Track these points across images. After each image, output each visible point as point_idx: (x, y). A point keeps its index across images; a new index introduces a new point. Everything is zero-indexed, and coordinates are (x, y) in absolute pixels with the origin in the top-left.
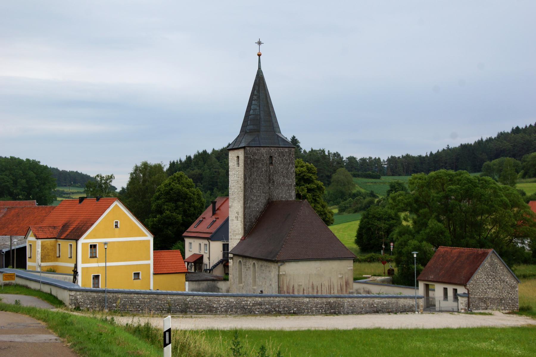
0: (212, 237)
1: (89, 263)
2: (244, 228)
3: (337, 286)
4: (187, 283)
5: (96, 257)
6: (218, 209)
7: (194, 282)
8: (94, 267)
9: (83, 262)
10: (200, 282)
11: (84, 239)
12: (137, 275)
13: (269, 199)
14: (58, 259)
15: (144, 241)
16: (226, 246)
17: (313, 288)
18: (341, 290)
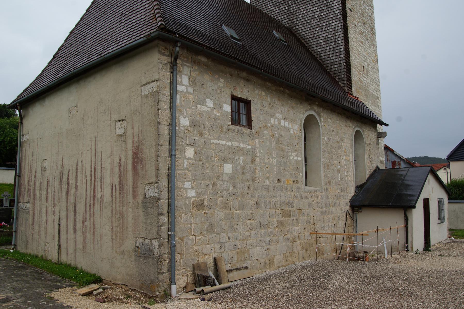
3: (112, 169)
17: (61, 181)
18: (121, 183)
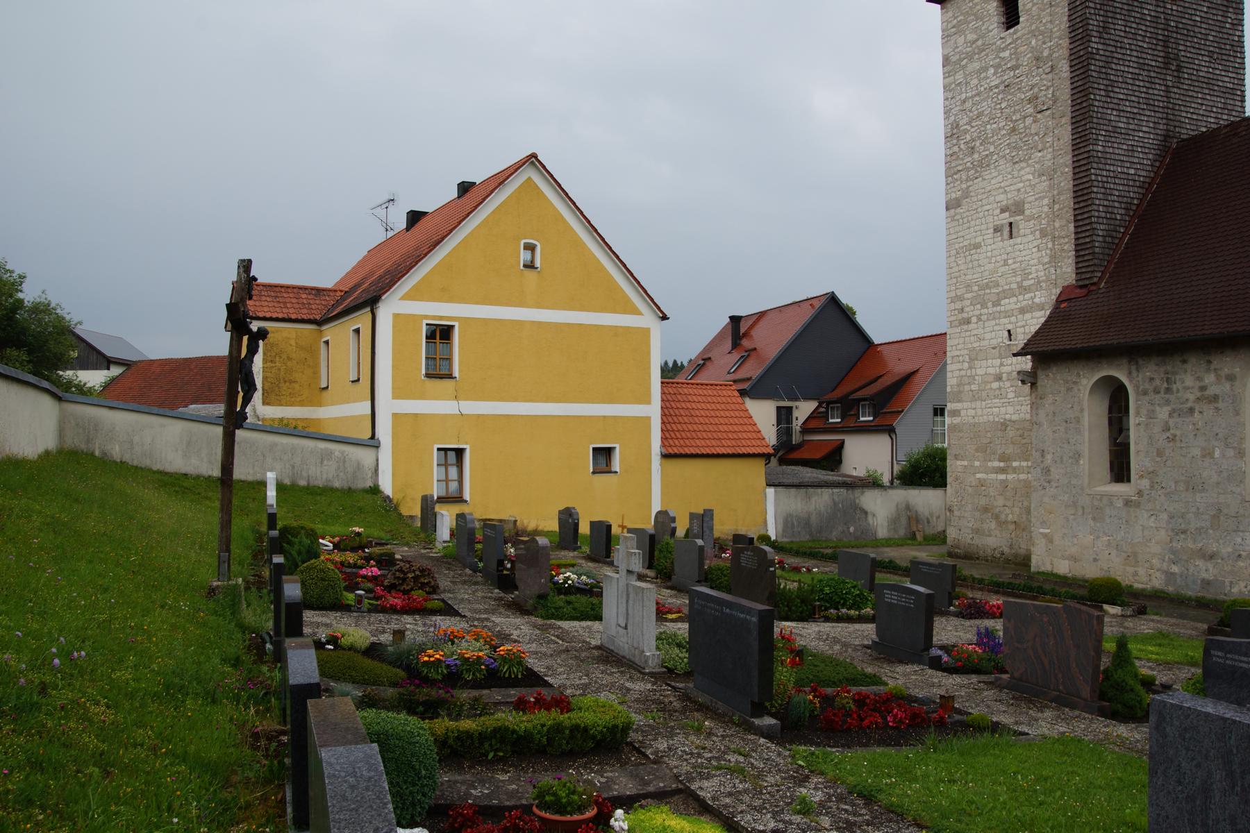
0: (753, 387)
1: (422, 396)
2: (1081, 249)
4: (771, 491)
5: (450, 376)
6: (745, 335)
7: (793, 491)
8: (444, 417)
9: (398, 394)
10: (811, 490)
11: (402, 298)
12: (603, 454)
13: (1166, 137)
14: (325, 393)
15: (627, 329)
16: (783, 412)
